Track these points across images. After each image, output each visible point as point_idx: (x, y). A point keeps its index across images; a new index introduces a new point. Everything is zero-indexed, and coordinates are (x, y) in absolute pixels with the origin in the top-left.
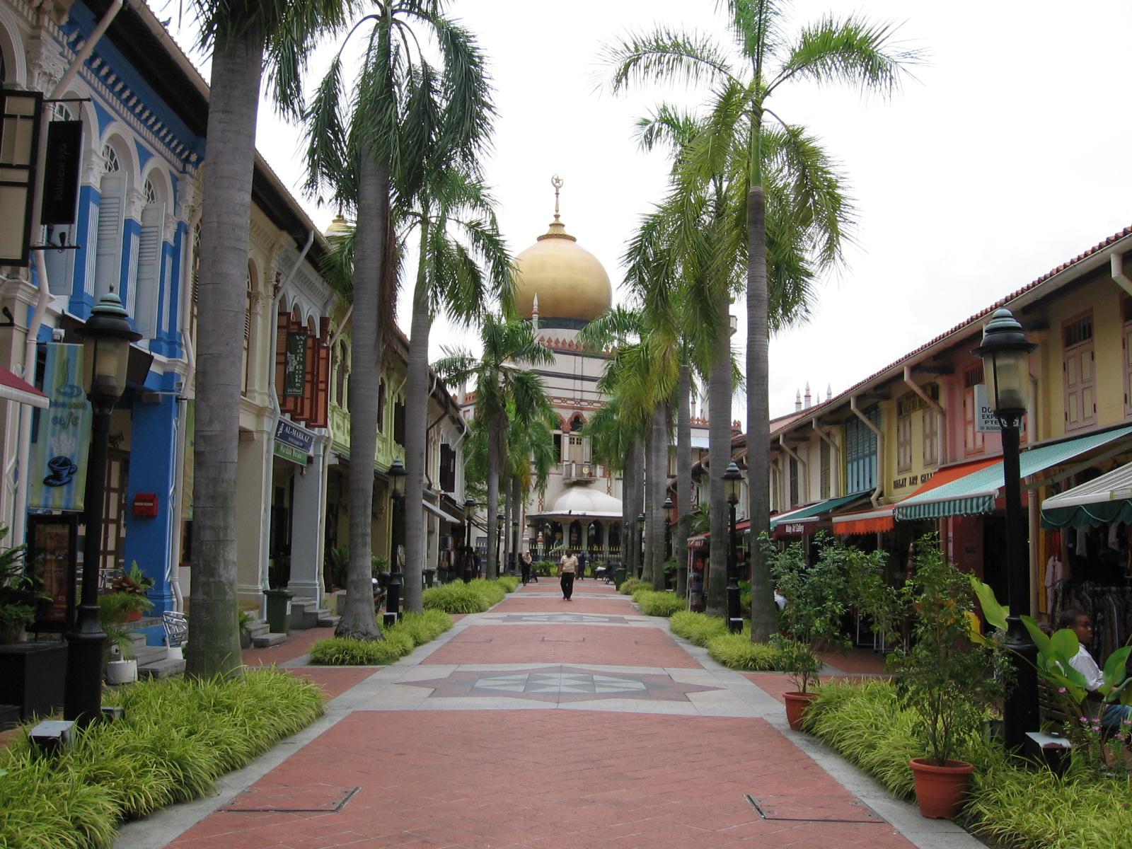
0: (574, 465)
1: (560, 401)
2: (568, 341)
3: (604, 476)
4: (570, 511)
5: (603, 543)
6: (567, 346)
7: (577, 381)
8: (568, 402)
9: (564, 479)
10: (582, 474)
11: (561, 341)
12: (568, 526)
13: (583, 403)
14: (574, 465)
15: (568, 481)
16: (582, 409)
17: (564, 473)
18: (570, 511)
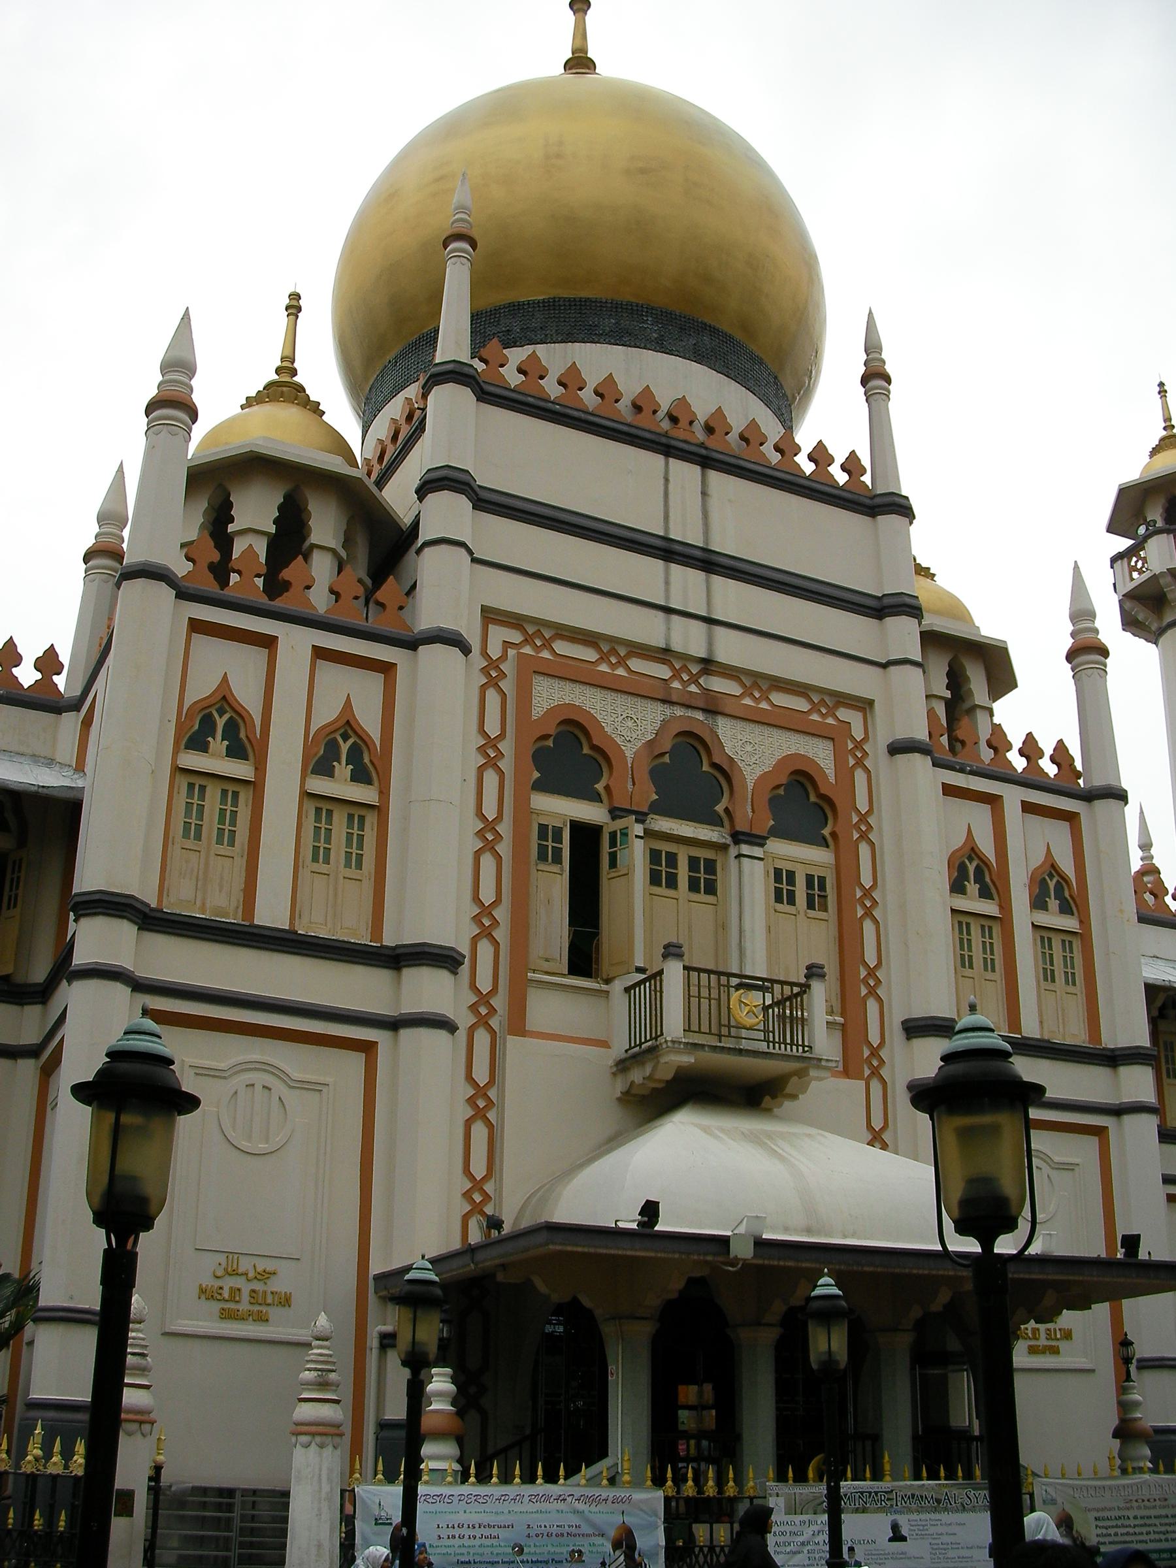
0: (674, 972)
1: (590, 655)
2: (629, 389)
3: (847, 1073)
4: (650, 1210)
5: (876, 1439)
6: (624, 406)
7: (676, 570)
8: (636, 664)
9: (623, 1066)
10: (726, 1026)
11: (592, 379)
12: (644, 1331)
13: (718, 685)
14: (674, 972)
15: (637, 1076)
16: (713, 707)
17: (620, 1045)
18: (650, 1210)
